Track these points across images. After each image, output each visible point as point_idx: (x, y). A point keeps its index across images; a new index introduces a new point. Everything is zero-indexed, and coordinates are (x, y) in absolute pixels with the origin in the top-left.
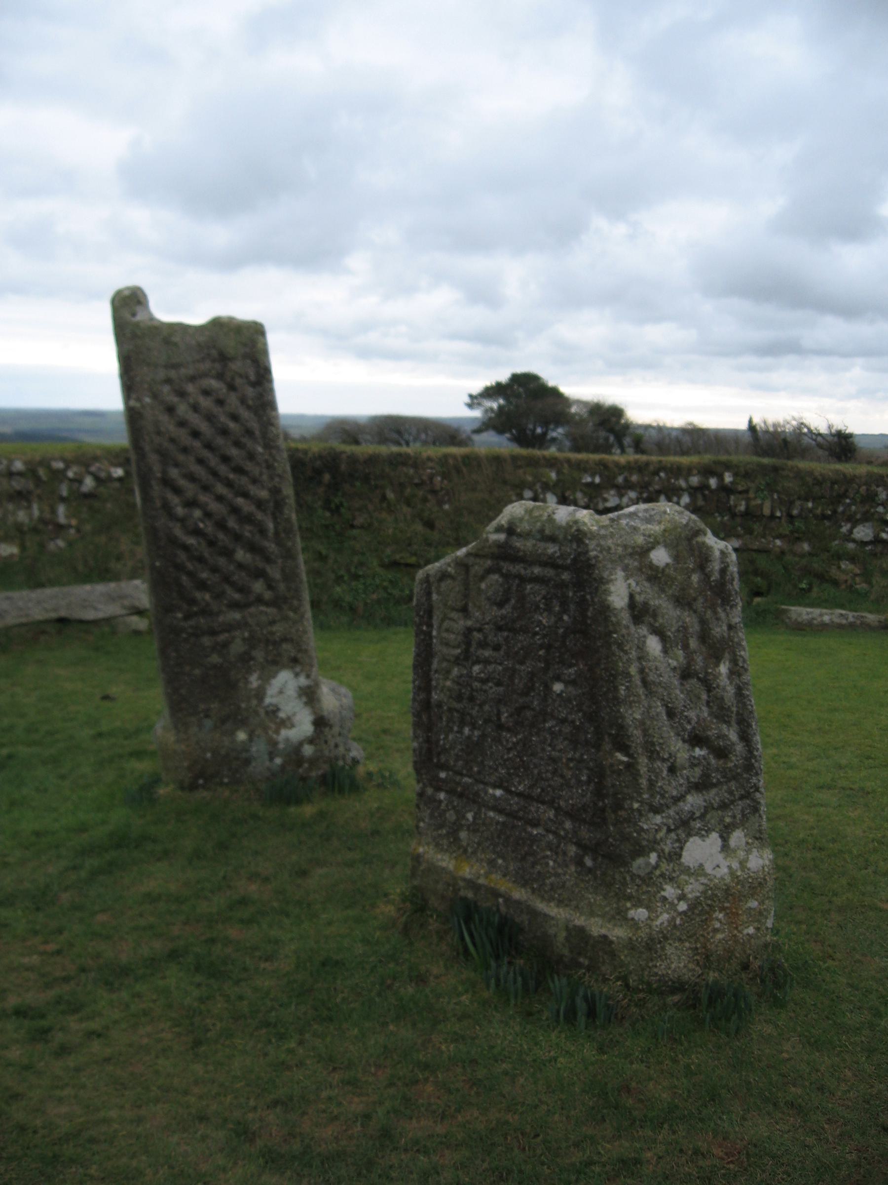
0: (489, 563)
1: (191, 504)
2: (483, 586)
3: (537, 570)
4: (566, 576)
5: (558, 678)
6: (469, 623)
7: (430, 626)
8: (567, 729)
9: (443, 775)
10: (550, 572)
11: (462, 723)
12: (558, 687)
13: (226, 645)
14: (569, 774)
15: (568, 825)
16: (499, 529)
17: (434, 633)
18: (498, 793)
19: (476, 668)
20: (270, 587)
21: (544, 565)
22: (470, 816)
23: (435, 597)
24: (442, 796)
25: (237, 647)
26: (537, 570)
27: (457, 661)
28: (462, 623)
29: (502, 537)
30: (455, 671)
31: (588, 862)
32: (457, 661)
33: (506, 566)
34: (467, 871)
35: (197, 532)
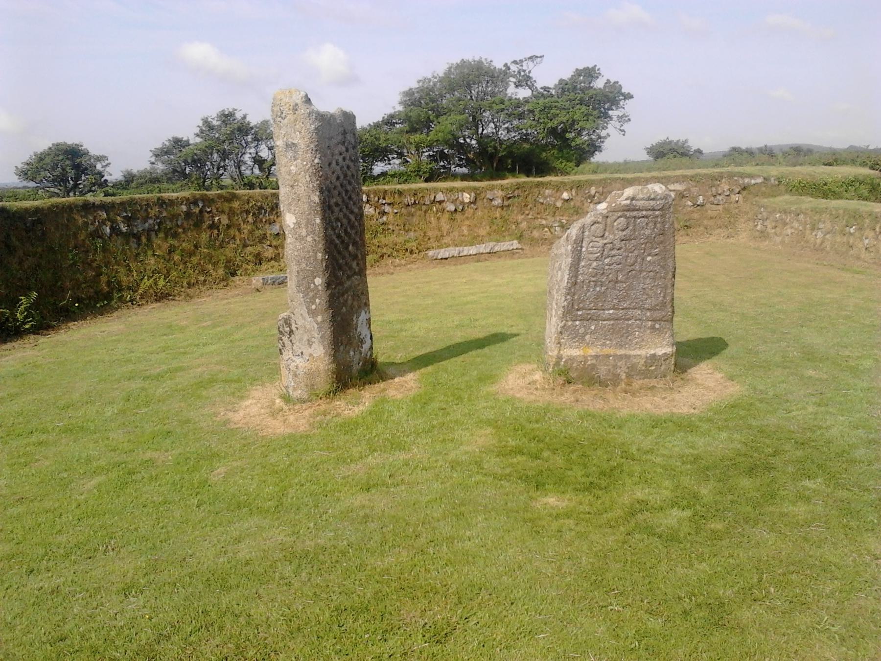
0: (620, 214)
1: (338, 219)
2: (615, 224)
3: (644, 213)
4: (657, 213)
5: (649, 255)
6: (605, 241)
7: (582, 247)
8: (652, 274)
9: (580, 313)
10: (650, 213)
11: (596, 286)
12: (649, 258)
13: (346, 301)
14: (650, 293)
15: (648, 314)
16: (626, 199)
17: (584, 249)
18: (611, 312)
19: (607, 261)
20: (358, 264)
21: (646, 210)
22: (593, 328)
23: (587, 233)
24: (577, 323)
25: (350, 302)
26: (644, 213)
27: (597, 259)
28: (602, 242)
29: (628, 202)
30: (595, 264)
31: (657, 326)
32: (597, 259)
33: (628, 214)
34: (591, 352)
35: (339, 237)
